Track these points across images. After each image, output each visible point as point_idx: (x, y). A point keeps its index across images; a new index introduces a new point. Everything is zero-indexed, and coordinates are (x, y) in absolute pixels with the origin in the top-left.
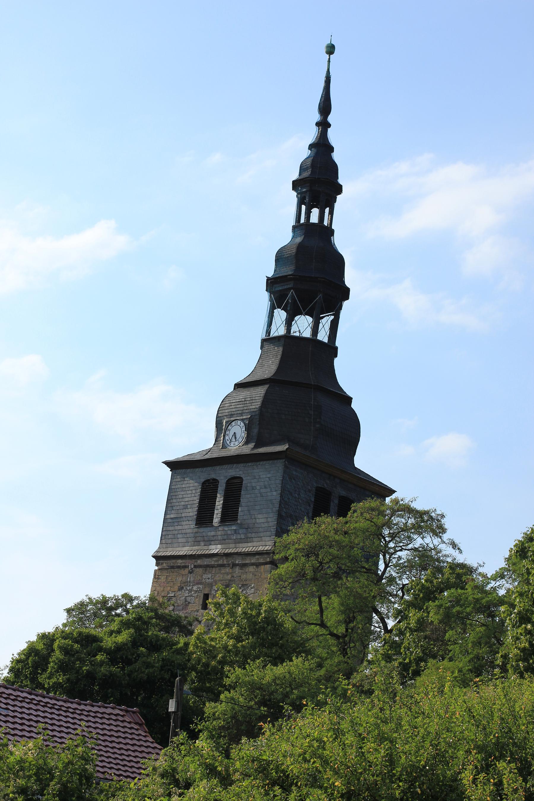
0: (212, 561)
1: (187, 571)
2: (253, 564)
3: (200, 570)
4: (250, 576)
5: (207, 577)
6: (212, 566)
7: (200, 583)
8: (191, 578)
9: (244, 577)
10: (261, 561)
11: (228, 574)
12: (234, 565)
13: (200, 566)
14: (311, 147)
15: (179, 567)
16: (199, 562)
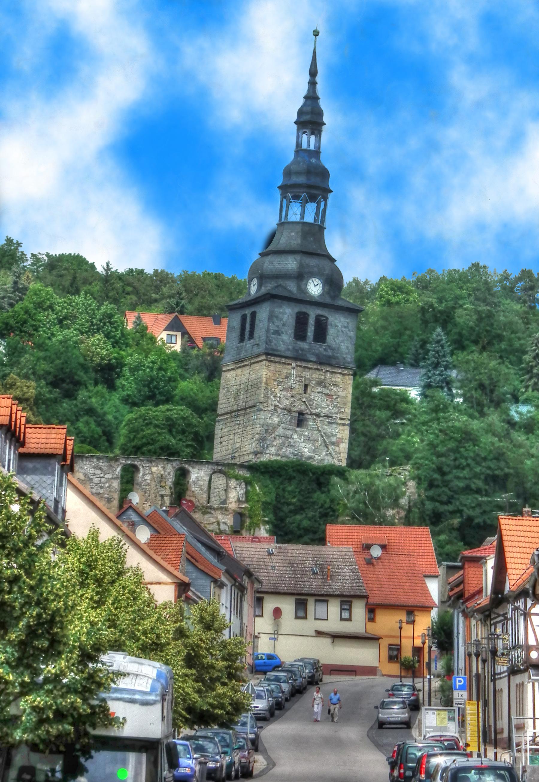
0: (310, 365)
1: (290, 367)
2: (340, 373)
3: (301, 369)
4: (339, 380)
5: (307, 374)
6: (310, 369)
7: (302, 377)
8: (294, 372)
9: (334, 379)
10: (346, 372)
11: (322, 375)
12: (327, 371)
13: (301, 366)
14: (306, 97)
15: (284, 363)
16: (298, 363)
